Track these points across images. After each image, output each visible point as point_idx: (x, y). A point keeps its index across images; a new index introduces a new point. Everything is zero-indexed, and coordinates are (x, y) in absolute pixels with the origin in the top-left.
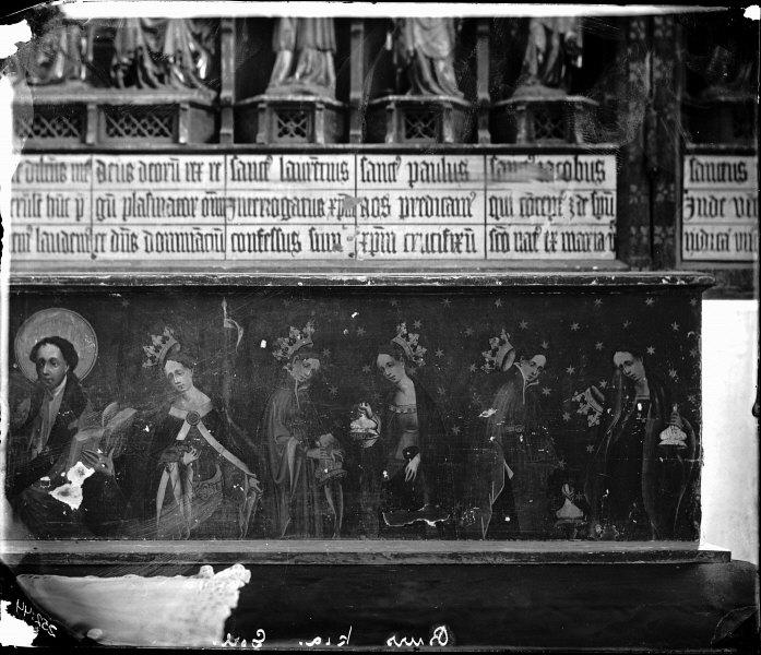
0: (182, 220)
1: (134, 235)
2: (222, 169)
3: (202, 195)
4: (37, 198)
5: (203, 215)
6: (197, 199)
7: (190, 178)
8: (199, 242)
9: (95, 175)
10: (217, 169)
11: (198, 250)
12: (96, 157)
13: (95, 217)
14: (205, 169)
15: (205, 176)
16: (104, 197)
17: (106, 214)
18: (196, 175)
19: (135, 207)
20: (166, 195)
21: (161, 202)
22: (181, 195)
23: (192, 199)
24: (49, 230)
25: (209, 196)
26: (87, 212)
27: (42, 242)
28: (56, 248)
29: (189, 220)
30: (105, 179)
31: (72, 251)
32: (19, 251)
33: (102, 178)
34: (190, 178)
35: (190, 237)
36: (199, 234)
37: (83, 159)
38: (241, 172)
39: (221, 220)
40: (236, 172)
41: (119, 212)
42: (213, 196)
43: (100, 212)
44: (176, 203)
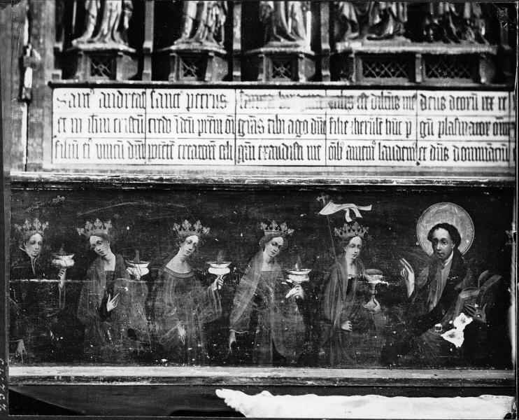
1: (445, 149)
3: (493, 120)
4: (379, 121)
5: (494, 134)
7: (485, 107)
13: (419, 135)
16: (425, 121)
22: (479, 120)
24: (387, 144)
25: (498, 121)
29: (485, 137)
30: (426, 108)
31: (403, 160)
34: (485, 107)
35: (485, 150)
39: (506, 138)
42: (501, 121)
43: (423, 132)
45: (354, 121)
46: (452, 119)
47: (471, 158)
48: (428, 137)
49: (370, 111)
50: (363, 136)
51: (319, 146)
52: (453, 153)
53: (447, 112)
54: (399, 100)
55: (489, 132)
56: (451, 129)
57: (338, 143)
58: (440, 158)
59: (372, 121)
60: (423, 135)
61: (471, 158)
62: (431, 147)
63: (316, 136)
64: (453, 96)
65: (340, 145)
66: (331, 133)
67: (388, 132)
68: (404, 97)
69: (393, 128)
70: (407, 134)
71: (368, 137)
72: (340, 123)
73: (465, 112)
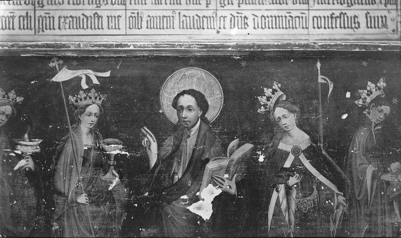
1: (245, 17)
8: (291, 22)
11: (290, 28)
13: (219, 5)
24: (187, 13)
29: (284, 6)
31: (203, 29)
32: (167, 28)
35: (284, 18)
36: (290, 16)
39: (305, 7)
50: (163, 6)
51: (119, 16)
57: (138, 13)
60: (223, 5)
65: (140, 15)
66: (131, 4)
70: (207, 4)
71: (168, 6)
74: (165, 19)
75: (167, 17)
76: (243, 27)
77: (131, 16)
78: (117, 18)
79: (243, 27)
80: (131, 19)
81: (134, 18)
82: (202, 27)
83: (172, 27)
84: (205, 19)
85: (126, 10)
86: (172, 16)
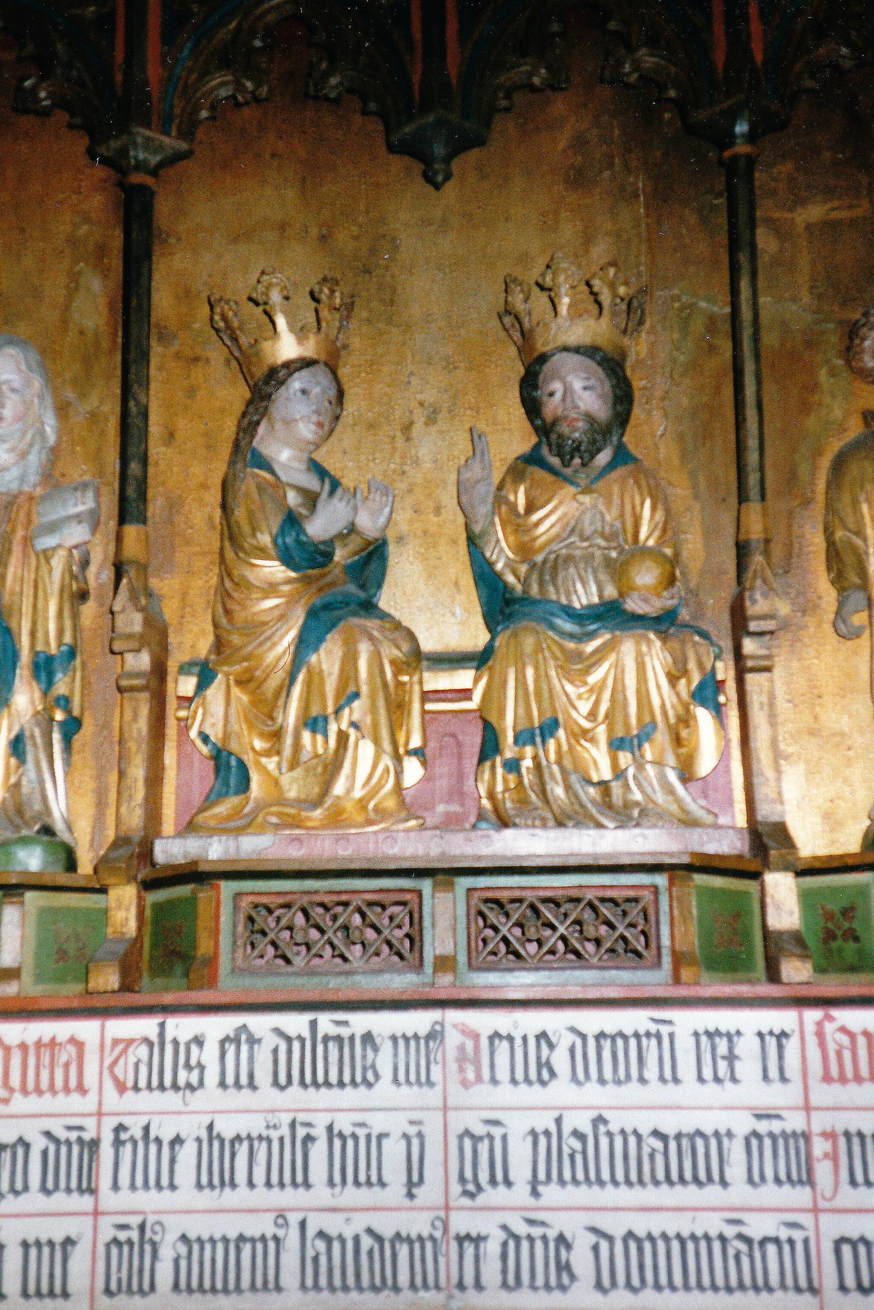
0: (690, 1195)
1: (561, 1239)
2: (792, 1047)
3: (743, 1124)
4: (301, 1132)
5: (750, 1181)
6: (730, 1134)
7: (708, 1073)
8: (745, 1261)
9: (452, 1066)
10: (780, 1048)
11: (741, 1286)
12: (453, 1016)
13: (456, 1188)
14: (747, 1047)
15: (748, 1068)
16: (480, 1130)
17: (484, 1177)
18: (722, 1065)
19: (566, 1156)
20: (645, 1123)
21: (632, 1141)
22: (687, 1122)
23: (717, 1134)
24: (334, 1225)
25: (763, 1127)
26: (433, 1172)
27: (316, 1259)
28: (351, 1280)
29: (712, 1194)
30: (479, 1078)
31: (396, 1288)
32: (253, 1287)
33: (471, 1075)
34: (708, 1073)
35: (717, 1246)
36: (741, 1237)
37: (419, 1021)
38: (847, 1055)
39: (801, 1196)
40: (832, 1057)
41: (520, 1171)
42: (776, 1126)
43: (468, 1174)
44: (673, 1146)
45: (204, 1135)
46: (583, 1122)
47: (663, 1279)
48: (492, 1196)
49: (267, 1095)
50: (241, 1196)
51: (69, 1242)
52: (590, 1255)
53: (562, 1091)
54: (376, 1050)
55: (729, 1173)
56: (579, 1158)
57: (142, 1227)
58: (540, 1281)
59: (275, 1135)
60: (471, 1187)
61: (663, 1279)
62: (502, 1235)
63: (60, 1201)
64: (583, 1029)
65: (148, 1234)
66: (115, 1187)
67: (337, 1178)
68: (394, 1039)
69: (354, 1159)
70: (410, 1184)
71: (262, 1197)
72: (153, 1148)
73: (632, 1092)
74: (247, 1250)
75: (253, 1240)
76: (553, 1281)
77: (115, 1241)
78: (58, 1248)
79: (553, 1281)
80: (114, 1251)
81: (126, 1249)
82: (390, 1282)
83: (271, 1285)
84: (403, 1251)
85: (96, 1213)
86: (276, 1239)
